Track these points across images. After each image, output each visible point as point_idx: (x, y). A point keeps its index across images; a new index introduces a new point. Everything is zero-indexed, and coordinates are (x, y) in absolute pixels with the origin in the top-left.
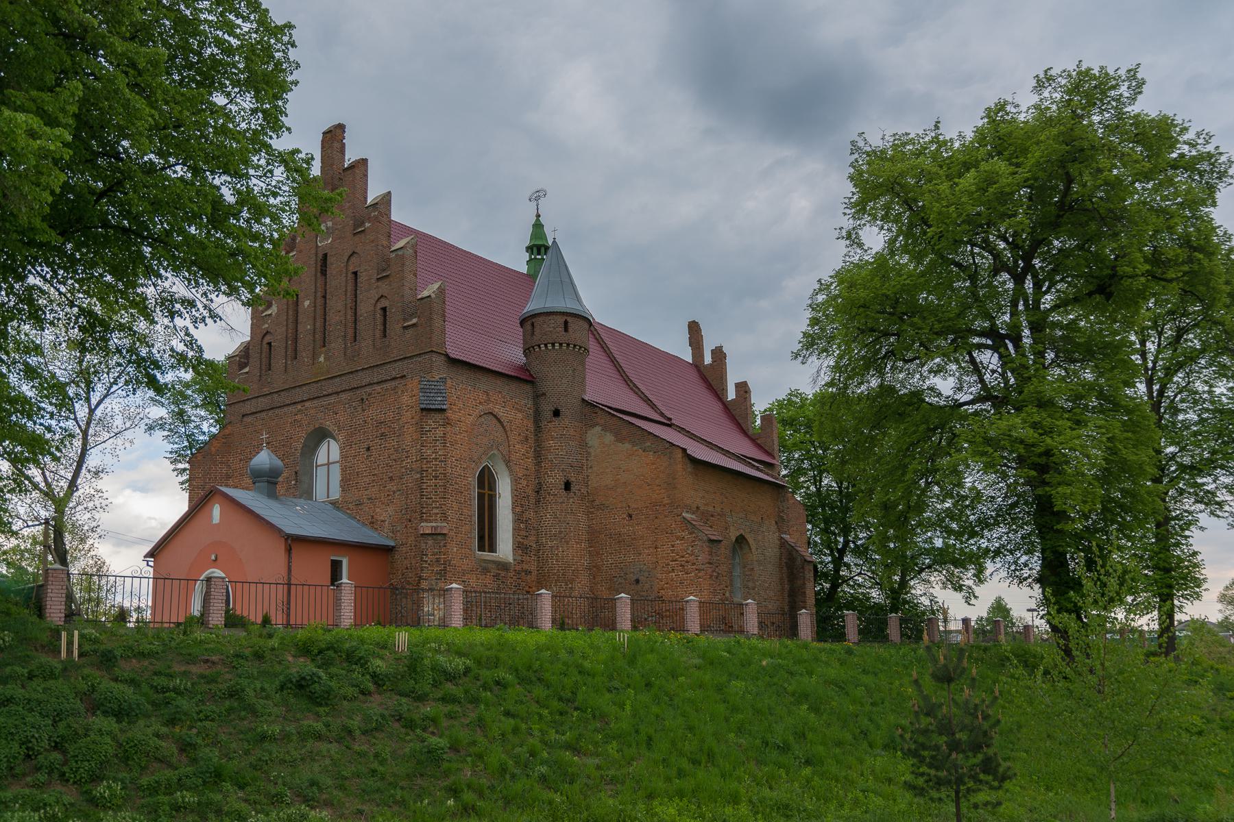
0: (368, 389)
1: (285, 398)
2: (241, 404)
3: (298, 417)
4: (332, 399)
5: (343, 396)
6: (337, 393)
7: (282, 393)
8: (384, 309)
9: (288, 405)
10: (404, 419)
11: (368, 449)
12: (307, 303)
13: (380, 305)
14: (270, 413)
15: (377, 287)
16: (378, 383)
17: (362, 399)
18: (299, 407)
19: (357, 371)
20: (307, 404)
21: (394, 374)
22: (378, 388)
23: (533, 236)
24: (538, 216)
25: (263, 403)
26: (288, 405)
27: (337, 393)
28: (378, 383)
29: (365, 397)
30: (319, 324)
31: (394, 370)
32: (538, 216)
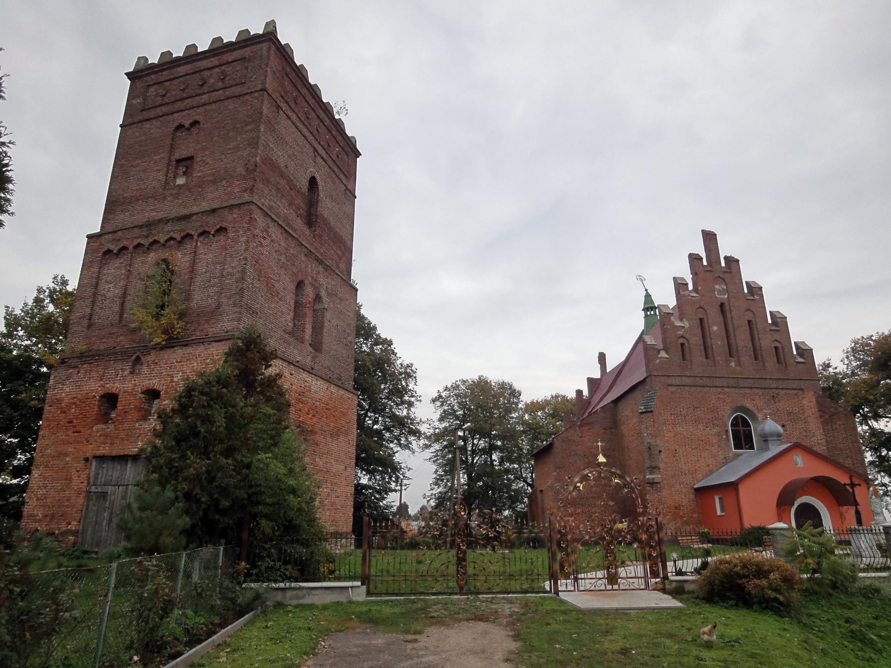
2: (666, 377)
3: (722, 396)
4: (747, 391)
8: (776, 348)
10: (806, 414)
12: (715, 328)
13: (773, 345)
15: (771, 334)
17: (773, 396)
18: (719, 390)
19: (766, 379)
20: (726, 390)
21: (794, 387)
22: (783, 392)
23: (645, 303)
24: (646, 290)
25: (686, 381)
27: (751, 388)
29: (775, 396)
30: (726, 343)
31: (795, 384)
32: (646, 290)
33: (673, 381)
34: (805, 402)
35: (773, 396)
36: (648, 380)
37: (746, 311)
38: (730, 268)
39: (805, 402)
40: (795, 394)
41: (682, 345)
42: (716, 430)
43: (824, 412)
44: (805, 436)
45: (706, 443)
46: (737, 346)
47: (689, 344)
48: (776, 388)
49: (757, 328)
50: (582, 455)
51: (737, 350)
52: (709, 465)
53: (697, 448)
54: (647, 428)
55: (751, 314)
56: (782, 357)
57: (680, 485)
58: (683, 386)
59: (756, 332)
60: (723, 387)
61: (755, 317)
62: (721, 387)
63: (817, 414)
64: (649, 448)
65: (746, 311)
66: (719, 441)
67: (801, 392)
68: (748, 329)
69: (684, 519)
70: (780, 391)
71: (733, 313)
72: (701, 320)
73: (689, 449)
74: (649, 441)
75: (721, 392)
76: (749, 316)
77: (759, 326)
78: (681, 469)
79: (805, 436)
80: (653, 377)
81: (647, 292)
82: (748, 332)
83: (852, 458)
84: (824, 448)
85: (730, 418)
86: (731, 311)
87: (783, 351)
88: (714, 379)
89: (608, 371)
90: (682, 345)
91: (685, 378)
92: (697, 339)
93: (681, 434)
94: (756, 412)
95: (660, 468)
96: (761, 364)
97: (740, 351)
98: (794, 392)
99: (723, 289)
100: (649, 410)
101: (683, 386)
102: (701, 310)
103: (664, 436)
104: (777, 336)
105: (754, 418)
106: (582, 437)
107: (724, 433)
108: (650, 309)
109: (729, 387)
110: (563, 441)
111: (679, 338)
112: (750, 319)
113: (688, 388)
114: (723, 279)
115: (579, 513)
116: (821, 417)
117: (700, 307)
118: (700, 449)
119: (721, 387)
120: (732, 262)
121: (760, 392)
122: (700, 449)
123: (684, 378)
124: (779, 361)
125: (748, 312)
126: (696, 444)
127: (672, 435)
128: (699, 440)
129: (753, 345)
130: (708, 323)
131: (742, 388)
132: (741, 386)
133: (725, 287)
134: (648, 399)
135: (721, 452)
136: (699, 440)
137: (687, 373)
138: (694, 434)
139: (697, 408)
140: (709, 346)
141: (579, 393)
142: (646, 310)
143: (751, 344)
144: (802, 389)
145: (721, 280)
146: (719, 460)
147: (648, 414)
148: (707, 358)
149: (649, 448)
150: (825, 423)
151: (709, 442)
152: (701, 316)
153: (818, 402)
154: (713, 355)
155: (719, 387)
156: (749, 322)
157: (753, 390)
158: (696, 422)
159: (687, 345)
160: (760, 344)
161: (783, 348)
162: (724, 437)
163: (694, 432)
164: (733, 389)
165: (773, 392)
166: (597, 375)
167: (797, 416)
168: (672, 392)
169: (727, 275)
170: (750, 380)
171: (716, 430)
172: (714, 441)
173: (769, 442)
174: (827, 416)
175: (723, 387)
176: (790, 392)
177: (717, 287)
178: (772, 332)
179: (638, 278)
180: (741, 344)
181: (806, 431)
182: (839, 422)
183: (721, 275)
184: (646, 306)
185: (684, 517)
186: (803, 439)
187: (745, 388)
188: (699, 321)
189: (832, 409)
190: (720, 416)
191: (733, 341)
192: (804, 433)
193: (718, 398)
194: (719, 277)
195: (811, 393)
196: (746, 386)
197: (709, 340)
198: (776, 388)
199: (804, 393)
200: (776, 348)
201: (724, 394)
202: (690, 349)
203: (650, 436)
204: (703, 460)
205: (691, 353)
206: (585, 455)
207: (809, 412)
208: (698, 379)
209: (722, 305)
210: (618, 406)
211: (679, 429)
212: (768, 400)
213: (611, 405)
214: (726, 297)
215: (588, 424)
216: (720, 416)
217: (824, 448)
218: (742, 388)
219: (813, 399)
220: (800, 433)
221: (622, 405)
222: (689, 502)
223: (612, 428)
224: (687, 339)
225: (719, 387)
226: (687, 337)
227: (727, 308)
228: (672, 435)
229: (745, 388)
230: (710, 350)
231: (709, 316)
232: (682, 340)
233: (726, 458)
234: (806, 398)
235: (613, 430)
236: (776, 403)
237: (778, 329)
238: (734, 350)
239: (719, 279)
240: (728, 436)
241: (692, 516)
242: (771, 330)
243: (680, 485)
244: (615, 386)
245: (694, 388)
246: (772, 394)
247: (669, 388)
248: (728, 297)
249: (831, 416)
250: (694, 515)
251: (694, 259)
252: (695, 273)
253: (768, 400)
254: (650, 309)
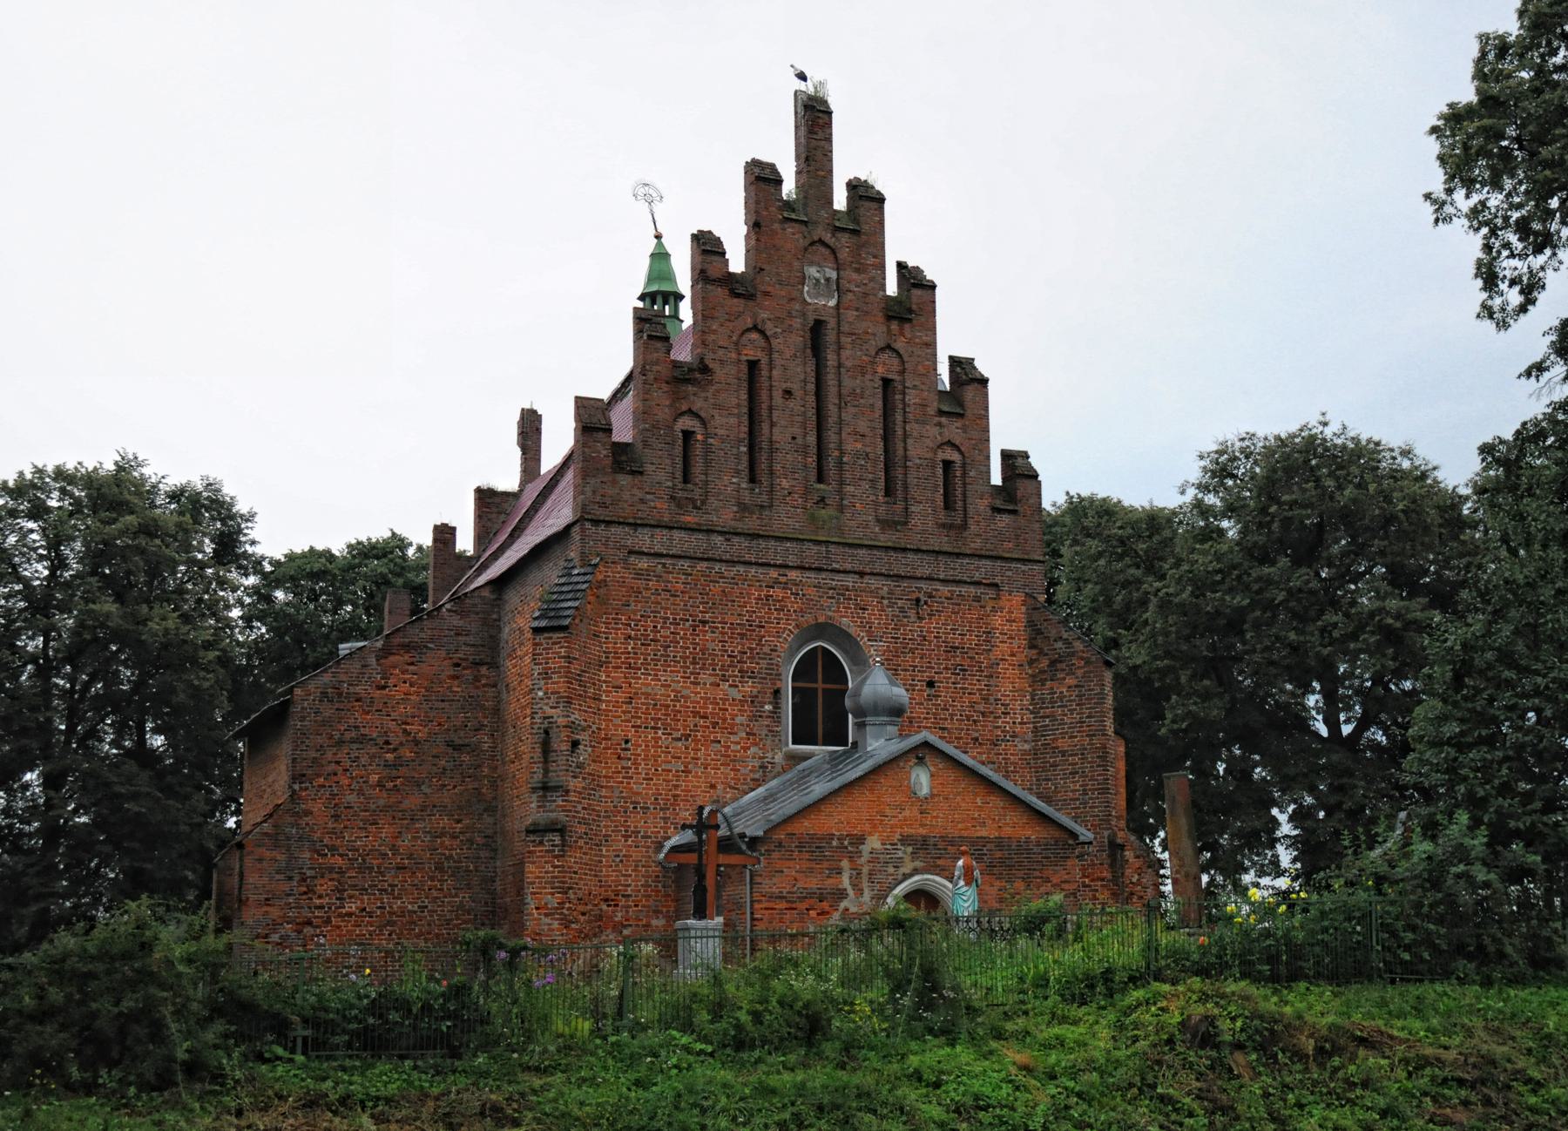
0: (923, 585)
1: (740, 546)
3: (777, 592)
4: (850, 581)
5: (874, 582)
6: (862, 574)
7: (736, 540)
8: (947, 465)
9: (749, 563)
11: (931, 684)
13: (941, 456)
14: (703, 565)
15: (940, 424)
16: (943, 581)
17: (918, 600)
18: (774, 573)
21: (977, 576)
22: (945, 590)
23: (651, 279)
24: (658, 237)
25: (680, 541)
26: (749, 563)
27: (862, 574)
28: (943, 581)
29: (923, 599)
30: (812, 439)
32: (658, 237)
33: (644, 539)
34: (997, 621)
35: (918, 600)
36: (576, 533)
37: (882, 350)
38: (856, 221)
39: (997, 621)
40: (977, 599)
41: (688, 435)
42: (749, 687)
43: (1041, 653)
44: (983, 714)
45: (715, 725)
46: (842, 453)
47: (707, 436)
48: (930, 579)
49: (905, 405)
50: (380, 741)
51: (840, 463)
52: (713, 786)
53: (687, 737)
54: (546, 675)
55: (896, 361)
56: (959, 492)
57: (626, 837)
58: (673, 556)
59: (899, 418)
60: (787, 567)
61: (902, 372)
62: (781, 566)
63: (1021, 657)
64: (546, 732)
65: (882, 350)
66: (754, 718)
67: (991, 593)
68: (879, 404)
69: (626, 932)
70: (938, 586)
71: (846, 353)
72: (753, 365)
73: (664, 740)
74: (550, 712)
75: (777, 582)
76: (886, 366)
77: (912, 398)
78: (640, 793)
79: (983, 714)
80: (588, 525)
81: (660, 244)
82: (878, 412)
83: (1084, 775)
84: (1027, 747)
85: (793, 655)
86: (840, 347)
87: (964, 474)
88: (763, 543)
89: (544, 470)
90: (688, 435)
91: (683, 534)
92: (733, 420)
93: (647, 695)
94: (864, 641)
95: (567, 792)
96: (900, 506)
97: (847, 467)
98: (972, 589)
99: (828, 280)
100: (555, 623)
101: (673, 556)
102: (754, 336)
103: (597, 699)
104: (953, 430)
105: (860, 661)
106: (384, 688)
107: (769, 697)
108: (659, 300)
109: (801, 568)
110: (324, 694)
111: (682, 414)
112: (890, 377)
113: (686, 564)
114: (833, 252)
115: (350, 914)
116: (1031, 662)
117: (755, 328)
118: (696, 741)
119: (781, 566)
120: (866, 197)
121: (884, 586)
122: (696, 741)
123: (677, 534)
124: (948, 505)
125: (885, 356)
126: (685, 727)
127: (621, 696)
128: (695, 714)
129: (886, 451)
130: (770, 377)
131: (839, 572)
132: (835, 566)
133: (834, 275)
134: (565, 589)
135: (753, 750)
136: (695, 714)
137: (690, 519)
138: (686, 697)
139: (704, 622)
140: (765, 445)
141: (445, 534)
142: (648, 300)
143: (880, 450)
144: (996, 585)
145: (826, 252)
146: (743, 771)
147: (556, 635)
148: (753, 479)
149: (546, 732)
150: (1037, 679)
151: (725, 720)
152: (750, 353)
153: (1031, 623)
154: (771, 472)
155: (775, 566)
156: (886, 382)
157: (866, 579)
158: (694, 663)
159: (699, 437)
160: (906, 450)
161: (964, 465)
162: (768, 707)
163: (685, 692)
164: (812, 575)
165: (920, 589)
166: (508, 480)
167: (972, 658)
168: (639, 574)
169: (844, 243)
170: (862, 552)
171: (749, 687)
172: (739, 720)
173: (868, 728)
174: (1044, 663)
175: (787, 567)
176: (964, 589)
177: (812, 271)
178: (943, 420)
179: (641, 191)
180: (851, 445)
181: (986, 700)
182: (1070, 681)
183: (827, 237)
184: (654, 288)
185: (625, 927)
186: (975, 721)
187: (845, 572)
188: (744, 368)
189: (1059, 644)
190: (766, 649)
191: (831, 436)
192: (981, 708)
193: (767, 597)
194: (821, 241)
195: (1018, 598)
196: (848, 567)
197: (765, 427)
198: (930, 579)
199: (998, 598)
200: (947, 465)
201: (785, 586)
202: (708, 450)
203: (552, 701)
204: (700, 771)
205: (708, 463)
206: (387, 743)
207: (1002, 649)
208: (718, 539)
209: (817, 328)
210: (506, 597)
211: (644, 682)
212: (902, 610)
213: (486, 593)
214: (832, 303)
215: (407, 647)
216: (766, 649)
217: (1027, 747)
218: (839, 572)
219: (1020, 613)
220: (972, 705)
221: (513, 597)
222: (646, 885)
223: (481, 664)
224: (703, 422)
225: (775, 566)
226: (703, 414)
227: (830, 336)
228: (621, 696)
229: (845, 572)
230: (764, 457)
231: (775, 355)
232: (686, 423)
233: (763, 767)
234: (1002, 610)
235: (484, 670)
236: (920, 618)
237: (959, 410)
238: (831, 463)
239: (823, 250)
240: (777, 706)
241: (648, 926)
242: (941, 413)
243: (626, 837)
244: (528, 531)
245: (705, 564)
246: (914, 597)
247: (632, 559)
248: (838, 306)
249: (1053, 663)
250: (654, 922)
251: (761, 177)
252: (756, 226)
253: (902, 610)
254: (659, 300)
